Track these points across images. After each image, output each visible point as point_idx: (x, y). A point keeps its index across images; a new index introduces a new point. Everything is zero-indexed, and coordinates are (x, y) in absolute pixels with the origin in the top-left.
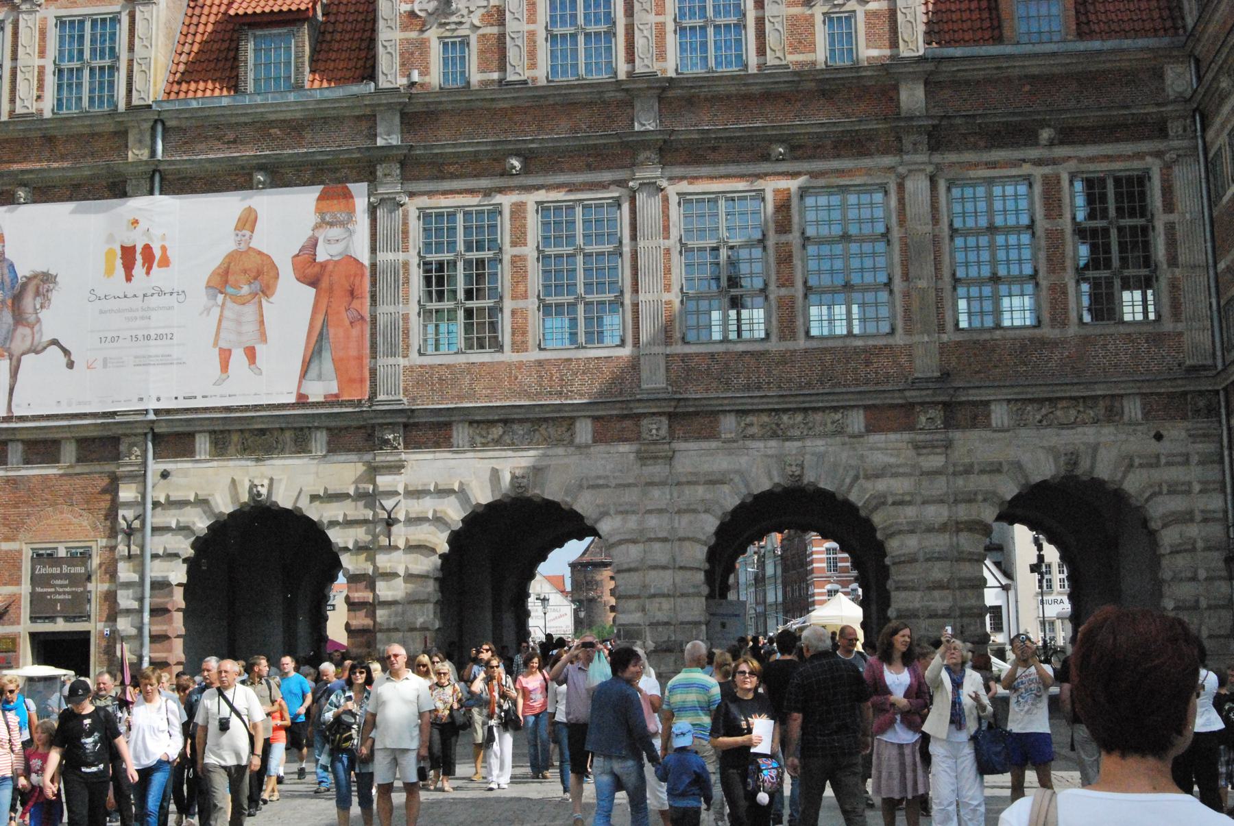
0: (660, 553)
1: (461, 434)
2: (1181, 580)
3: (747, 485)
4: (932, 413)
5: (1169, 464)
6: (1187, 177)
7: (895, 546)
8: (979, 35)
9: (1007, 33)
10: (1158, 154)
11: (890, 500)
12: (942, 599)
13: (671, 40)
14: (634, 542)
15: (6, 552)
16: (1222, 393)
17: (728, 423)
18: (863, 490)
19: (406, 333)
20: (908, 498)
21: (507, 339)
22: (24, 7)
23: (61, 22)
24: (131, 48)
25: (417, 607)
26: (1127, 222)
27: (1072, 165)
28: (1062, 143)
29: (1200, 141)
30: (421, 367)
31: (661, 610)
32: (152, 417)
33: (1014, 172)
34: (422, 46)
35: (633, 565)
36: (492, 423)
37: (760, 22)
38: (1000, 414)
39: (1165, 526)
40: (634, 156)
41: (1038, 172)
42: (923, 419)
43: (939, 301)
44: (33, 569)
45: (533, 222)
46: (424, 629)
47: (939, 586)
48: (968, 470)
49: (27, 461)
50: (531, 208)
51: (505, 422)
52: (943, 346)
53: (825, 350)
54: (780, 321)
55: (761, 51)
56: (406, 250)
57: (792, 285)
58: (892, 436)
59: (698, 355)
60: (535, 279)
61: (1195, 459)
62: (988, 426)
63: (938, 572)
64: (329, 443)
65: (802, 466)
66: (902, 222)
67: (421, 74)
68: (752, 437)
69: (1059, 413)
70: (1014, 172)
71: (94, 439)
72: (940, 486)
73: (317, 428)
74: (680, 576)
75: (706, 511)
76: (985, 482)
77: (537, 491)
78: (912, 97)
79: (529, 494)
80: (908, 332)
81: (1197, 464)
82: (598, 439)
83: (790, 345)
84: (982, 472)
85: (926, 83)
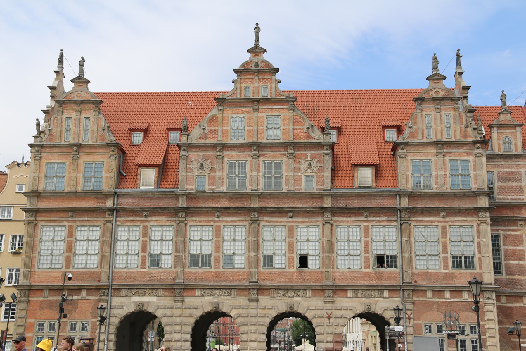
21: (213, 263)
75: (268, 317)
83: (292, 270)
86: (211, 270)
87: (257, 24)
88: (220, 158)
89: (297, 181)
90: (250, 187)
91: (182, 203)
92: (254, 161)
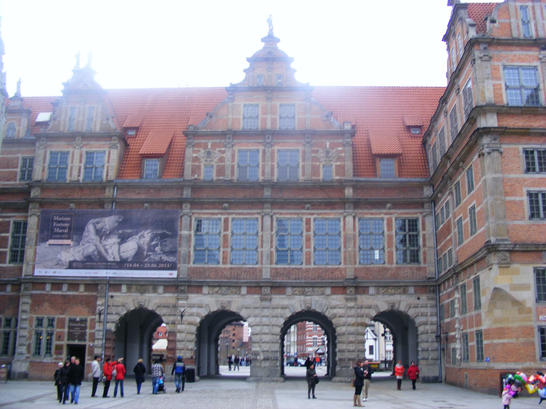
0: (266, 329)
1: (205, 290)
2: (424, 342)
3: (294, 309)
4: (351, 289)
5: (421, 307)
6: (429, 220)
7: (339, 330)
8: (369, 174)
9: (378, 173)
10: (421, 213)
11: (338, 316)
12: (352, 346)
14: (258, 325)
15: (61, 318)
16: (437, 287)
17: (289, 290)
18: (329, 312)
19: (189, 256)
20: (343, 315)
22: (77, 147)
23: (87, 153)
24: (108, 162)
25: (189, 343)
26: (411, 233)
27: (396, 215)
28: (393, 208)
29: (433, 210)
30: (194, 267)
31: (266, 347)
32: (108, 278)
33: (378, 216)
34: (199, 167)
35: (258, 333)
36: (215, 286)
37: (303, 166)
38: (372, 290)
39: (419, 326)
40: (263, 205)
41: (386, 217)
42: (348, 291)
43: (355, 255)
44: (69, 325)
46: (191, 350)
47: (351, 342)
49: (69, 290)
51: (219, 286)
52: (356, 269)
53: (320, 269)
54: (306, 259)
55: (303, 175)
56: (190, 230)
57: (310, 248)
58: (339, 296)
59: (280, 268)
61: (429, 306)
62: (368, 294)
63: (351, 338)
64: (164, 290)
65: (311, 304)
66: (344, 230)
67: (198, 176)
68: (296, 294)
69: (389, 290)
70: (378, 216)
71: (90, 284)
72: (353, 312)
73: (161, 285)
74: (272, 337)
75: (281, 317)
76: (366, 311)
77: (228, 308)
78: (349, 192)
79: (226, 309)
80: (345, 264)
81: (430, 307)
82: (248, 293)
83: (309, 266)
84: (366, 308)
85: (353, 188)
86: (218, 266)
87: (271, 16)
88: (229, 147)
90: (262, 178)
91: (187, 193)
92: (268, 150)
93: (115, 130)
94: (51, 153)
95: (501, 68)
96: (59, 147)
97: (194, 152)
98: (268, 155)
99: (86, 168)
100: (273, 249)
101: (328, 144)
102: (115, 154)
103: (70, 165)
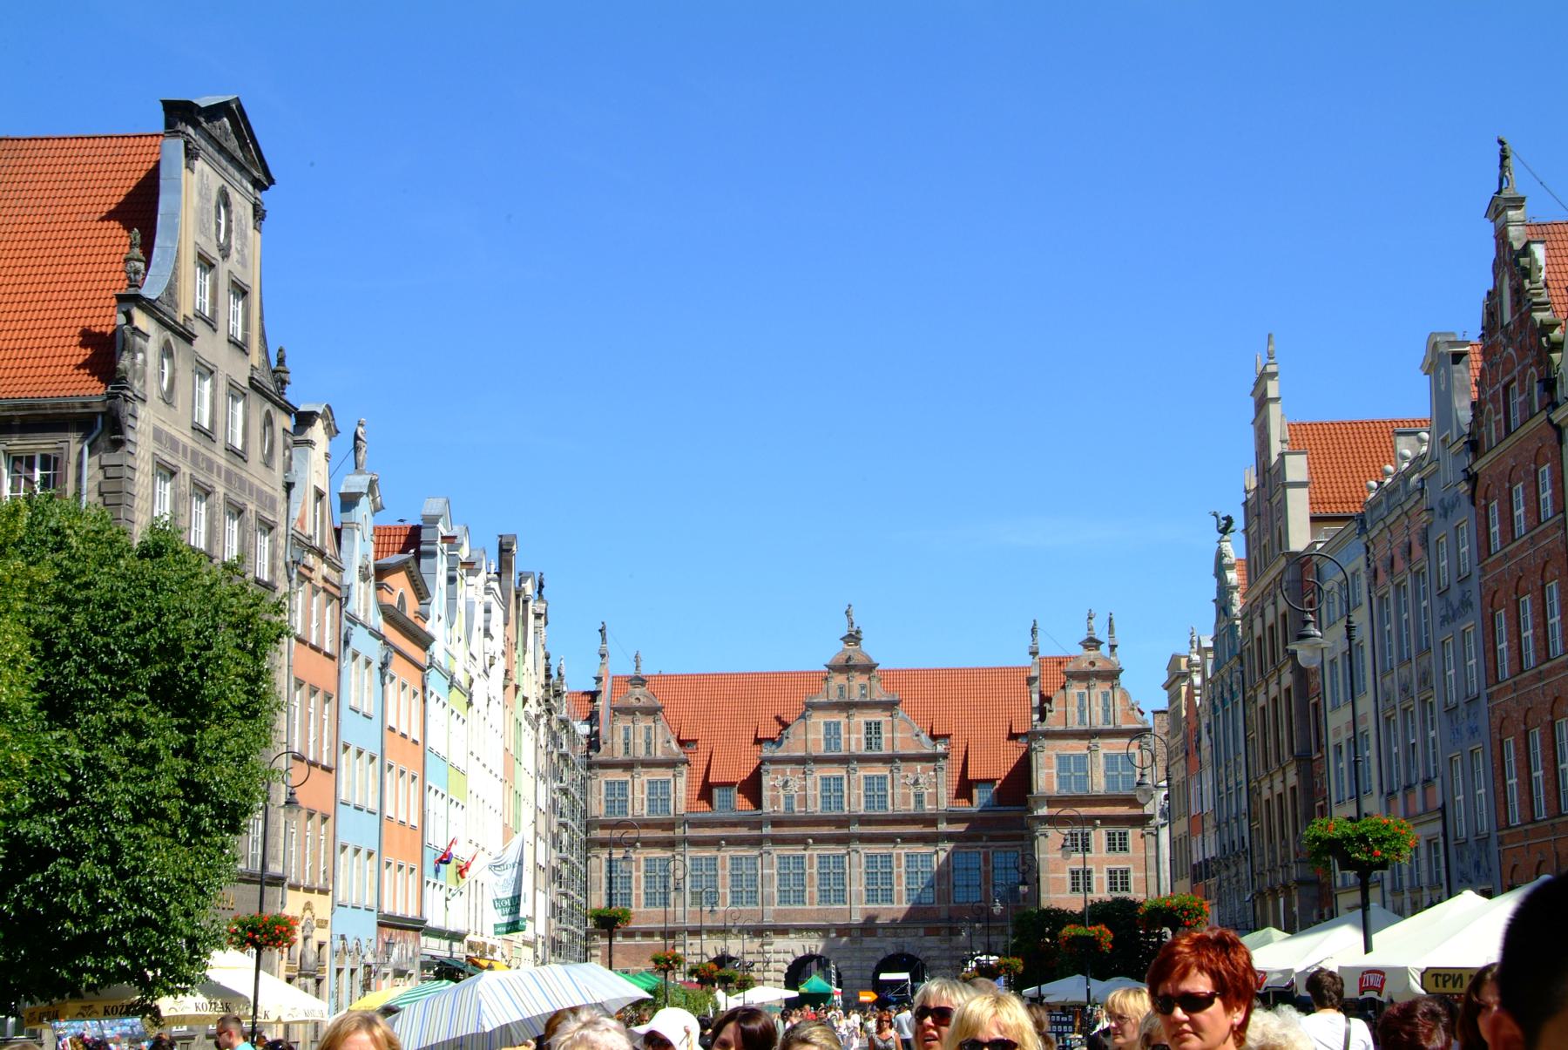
10: (1021, 846)
13: (863, 800)
23: (649, 782)
41: (982, 850)
42: (943, 932)
45: (816, 860)
48: (957, 949)
50: (815, 856)
52: (950, 909)
60: (816, 881)
72: (947, 953)
87: (850, 606)
89: (906, 802)
93: (679, 754)
94: (607, 783)
95: (1054, 756)
96: (617, 775)
97: (772, 779)
98: (852, 781)
99: (649, 800)
100: (863, 888)
101: (919, 767)
102: (682, 782)
103: (630, 797)
